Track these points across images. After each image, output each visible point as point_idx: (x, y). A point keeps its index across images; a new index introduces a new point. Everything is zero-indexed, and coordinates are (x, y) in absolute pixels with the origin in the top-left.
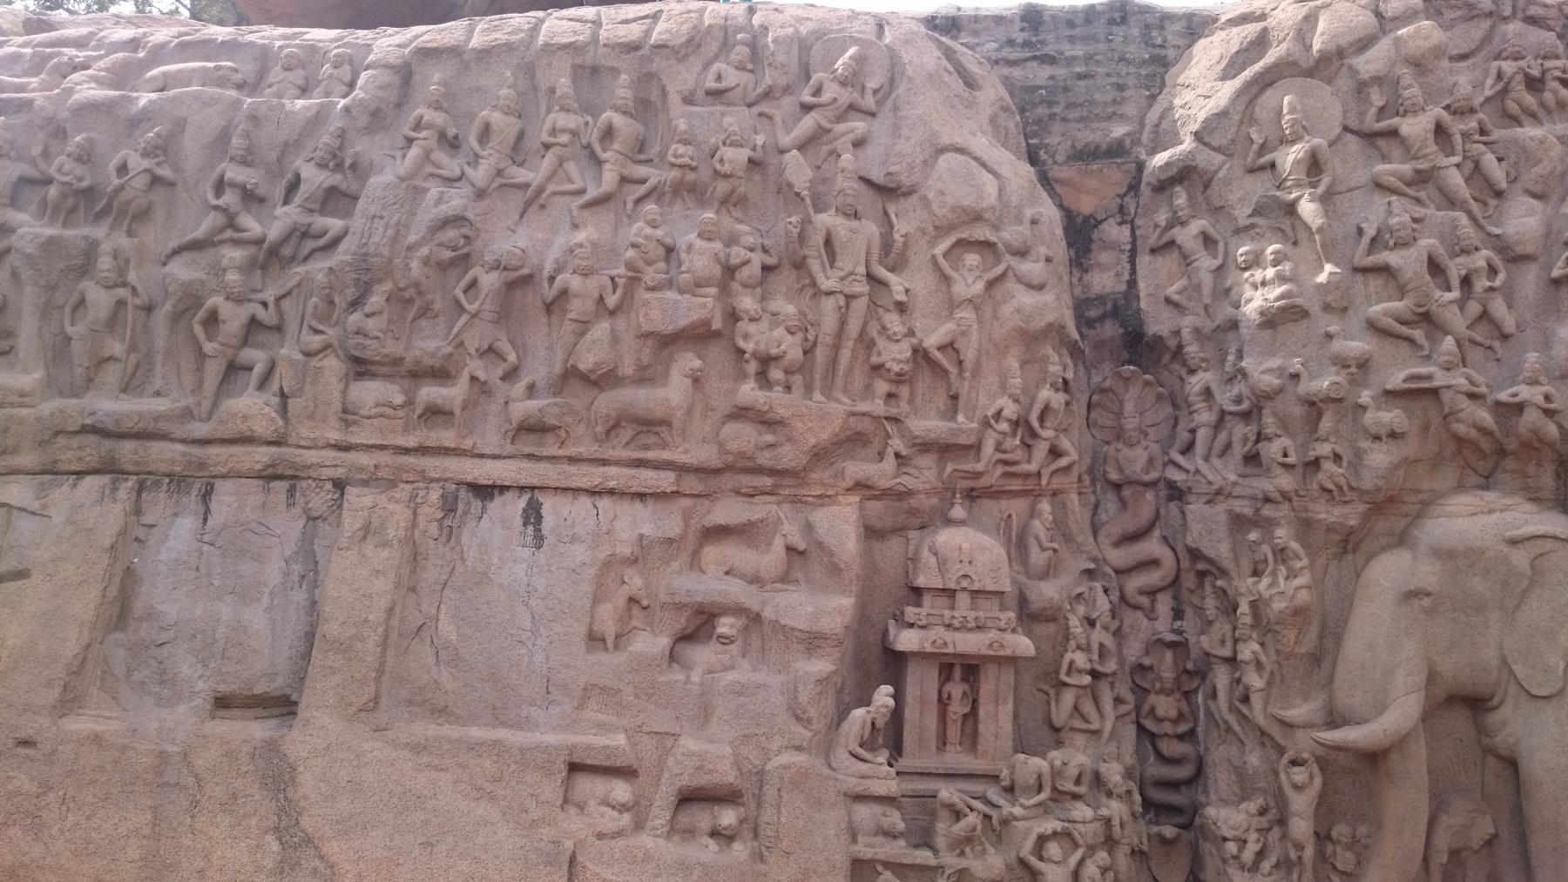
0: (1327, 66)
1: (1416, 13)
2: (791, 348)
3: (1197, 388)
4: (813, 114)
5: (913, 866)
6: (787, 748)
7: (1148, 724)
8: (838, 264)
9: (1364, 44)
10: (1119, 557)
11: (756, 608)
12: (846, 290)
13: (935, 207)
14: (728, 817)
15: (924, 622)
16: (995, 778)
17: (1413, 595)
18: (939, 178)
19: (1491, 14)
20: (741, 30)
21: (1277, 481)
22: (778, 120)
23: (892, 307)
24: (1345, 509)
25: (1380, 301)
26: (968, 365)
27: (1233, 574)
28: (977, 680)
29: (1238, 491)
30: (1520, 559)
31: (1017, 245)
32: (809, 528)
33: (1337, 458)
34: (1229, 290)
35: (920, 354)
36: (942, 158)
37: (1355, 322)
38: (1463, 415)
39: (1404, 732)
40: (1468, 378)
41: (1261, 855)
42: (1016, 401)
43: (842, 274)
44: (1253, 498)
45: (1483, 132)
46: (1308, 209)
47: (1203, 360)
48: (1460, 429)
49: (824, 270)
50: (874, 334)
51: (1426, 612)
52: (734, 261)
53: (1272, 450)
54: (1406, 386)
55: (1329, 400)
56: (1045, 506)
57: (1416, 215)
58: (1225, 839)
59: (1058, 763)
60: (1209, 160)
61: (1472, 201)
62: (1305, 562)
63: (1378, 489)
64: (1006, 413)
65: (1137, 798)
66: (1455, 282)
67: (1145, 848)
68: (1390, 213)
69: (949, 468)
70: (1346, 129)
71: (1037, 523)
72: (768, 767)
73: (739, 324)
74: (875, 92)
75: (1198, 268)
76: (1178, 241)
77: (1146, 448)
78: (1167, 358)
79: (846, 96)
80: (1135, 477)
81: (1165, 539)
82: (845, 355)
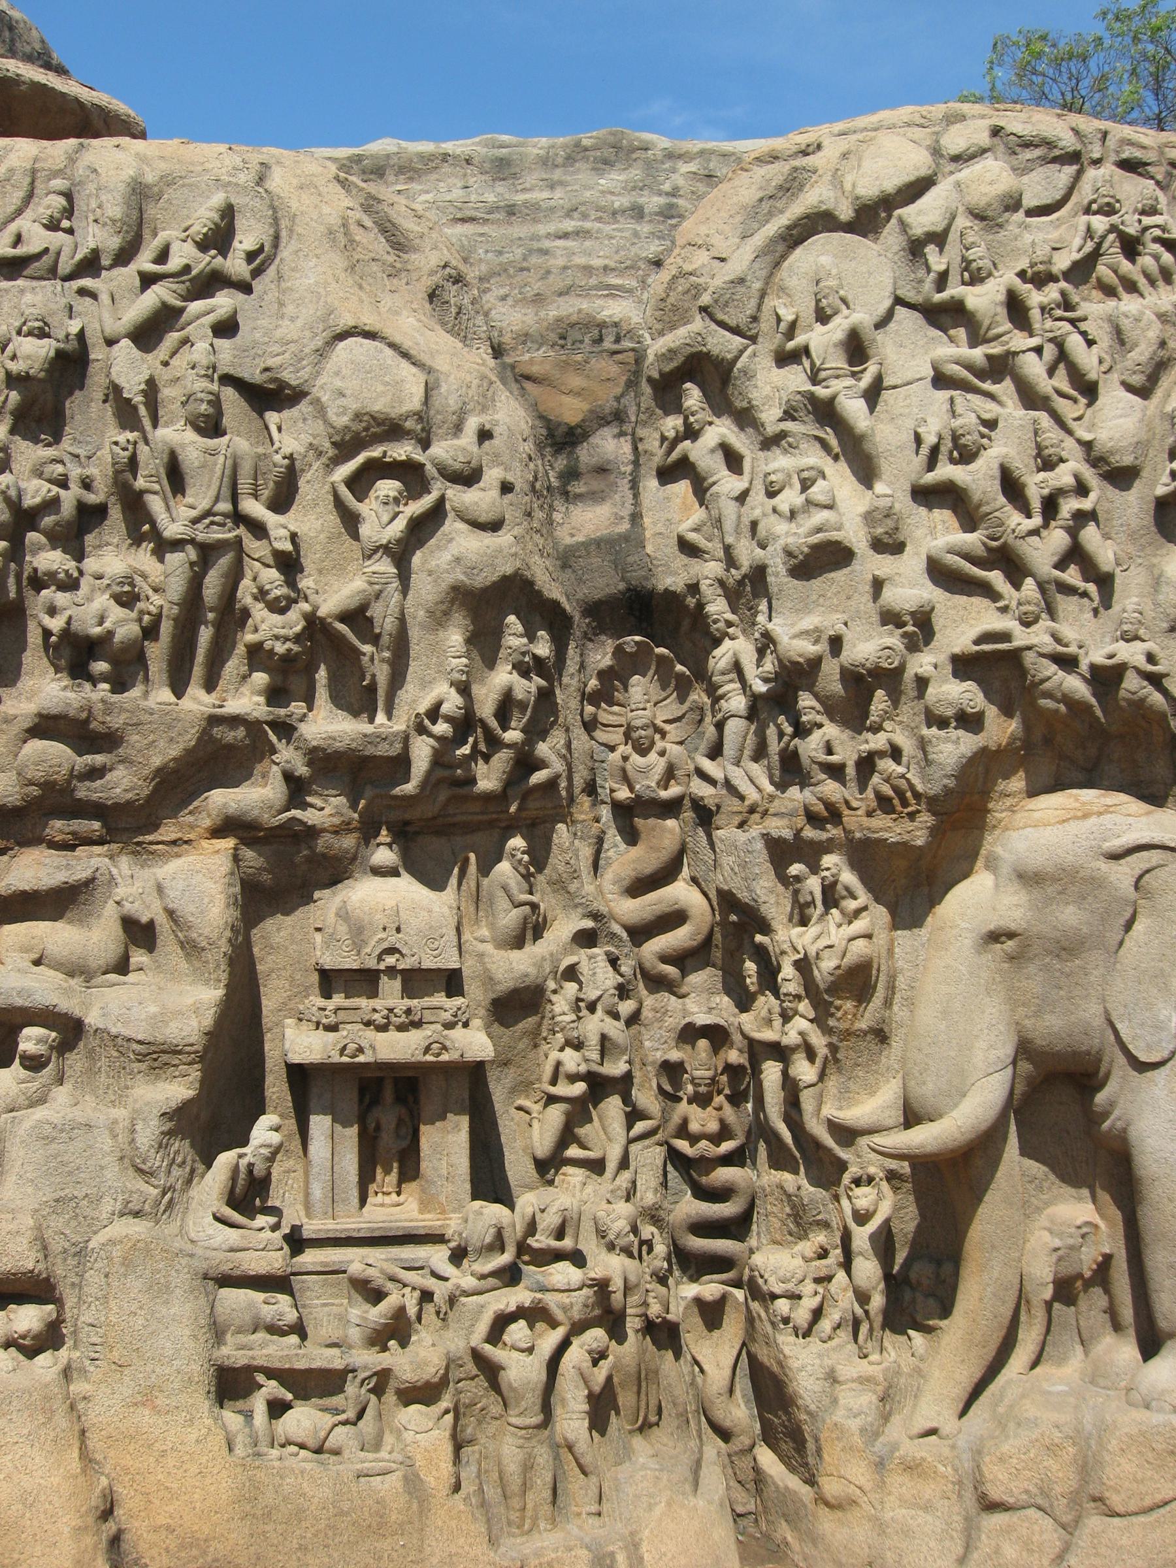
0: (868, 218)
1: (984, 151)
2: (123, 625)
3: (723, 664)
4: (155, 288)
5: (309, 1371)
6: (122, 1215)
7: (682, 1145)
8: (189, 500)
9: (917, 189)
10: (633, 909)
11: (77, 1012)
12: (201, 537)
13: (331, 414)
14: (27, 1318)
15: (332, 1020)
16: (437, 1239)
17: (994, 937)
18: (337, 374)
19: (1074, 157)
20: (56, 174)
21: (818, 789)
22: (104, 298)
23: (271, 561)
24: (910, 825)
26: (385, 640)
28: (416, 1101)
29: (775, 807)
30: (1122, 875)
31: (457, 466)
32: (160, 889)
33: (896, 753)
34: (754, 525)
35: (314, 625)
36: (342, 345)
38: (1047, 685)
39: (984, 1126)
41: (817, 1314)
42: (464, 689)
43: (194, 513)
44: (791, 815)
45: (1068, 305)
46: (854, 408)
47: (729, 624)
49: (168, 509)
50: (248, 600)
51: (1011, 958)
52: (29, 502)
53: (811, 747)
56: (517, 842)
57: (986, 416)
58: (774, 1297)
59: (529, 1211)
60: (723, 343)
61: (1055, 396)
62: (863, 897)
63: (948, 791)
64: (445, 708)
65: (660, 1249)
68: (954, 414)
69: (369, 792)
70: (899, 301)
71: (504, 867)
72: (91, 1245)
73: (44, 592)
74: (251, 256)
75: (718, 495)
76: (693, 457)
77: (662, 754)
78: (686, 623)
79: (203, 262)
80: (647, 794)
81: (694, 880)
82: (205, 635)
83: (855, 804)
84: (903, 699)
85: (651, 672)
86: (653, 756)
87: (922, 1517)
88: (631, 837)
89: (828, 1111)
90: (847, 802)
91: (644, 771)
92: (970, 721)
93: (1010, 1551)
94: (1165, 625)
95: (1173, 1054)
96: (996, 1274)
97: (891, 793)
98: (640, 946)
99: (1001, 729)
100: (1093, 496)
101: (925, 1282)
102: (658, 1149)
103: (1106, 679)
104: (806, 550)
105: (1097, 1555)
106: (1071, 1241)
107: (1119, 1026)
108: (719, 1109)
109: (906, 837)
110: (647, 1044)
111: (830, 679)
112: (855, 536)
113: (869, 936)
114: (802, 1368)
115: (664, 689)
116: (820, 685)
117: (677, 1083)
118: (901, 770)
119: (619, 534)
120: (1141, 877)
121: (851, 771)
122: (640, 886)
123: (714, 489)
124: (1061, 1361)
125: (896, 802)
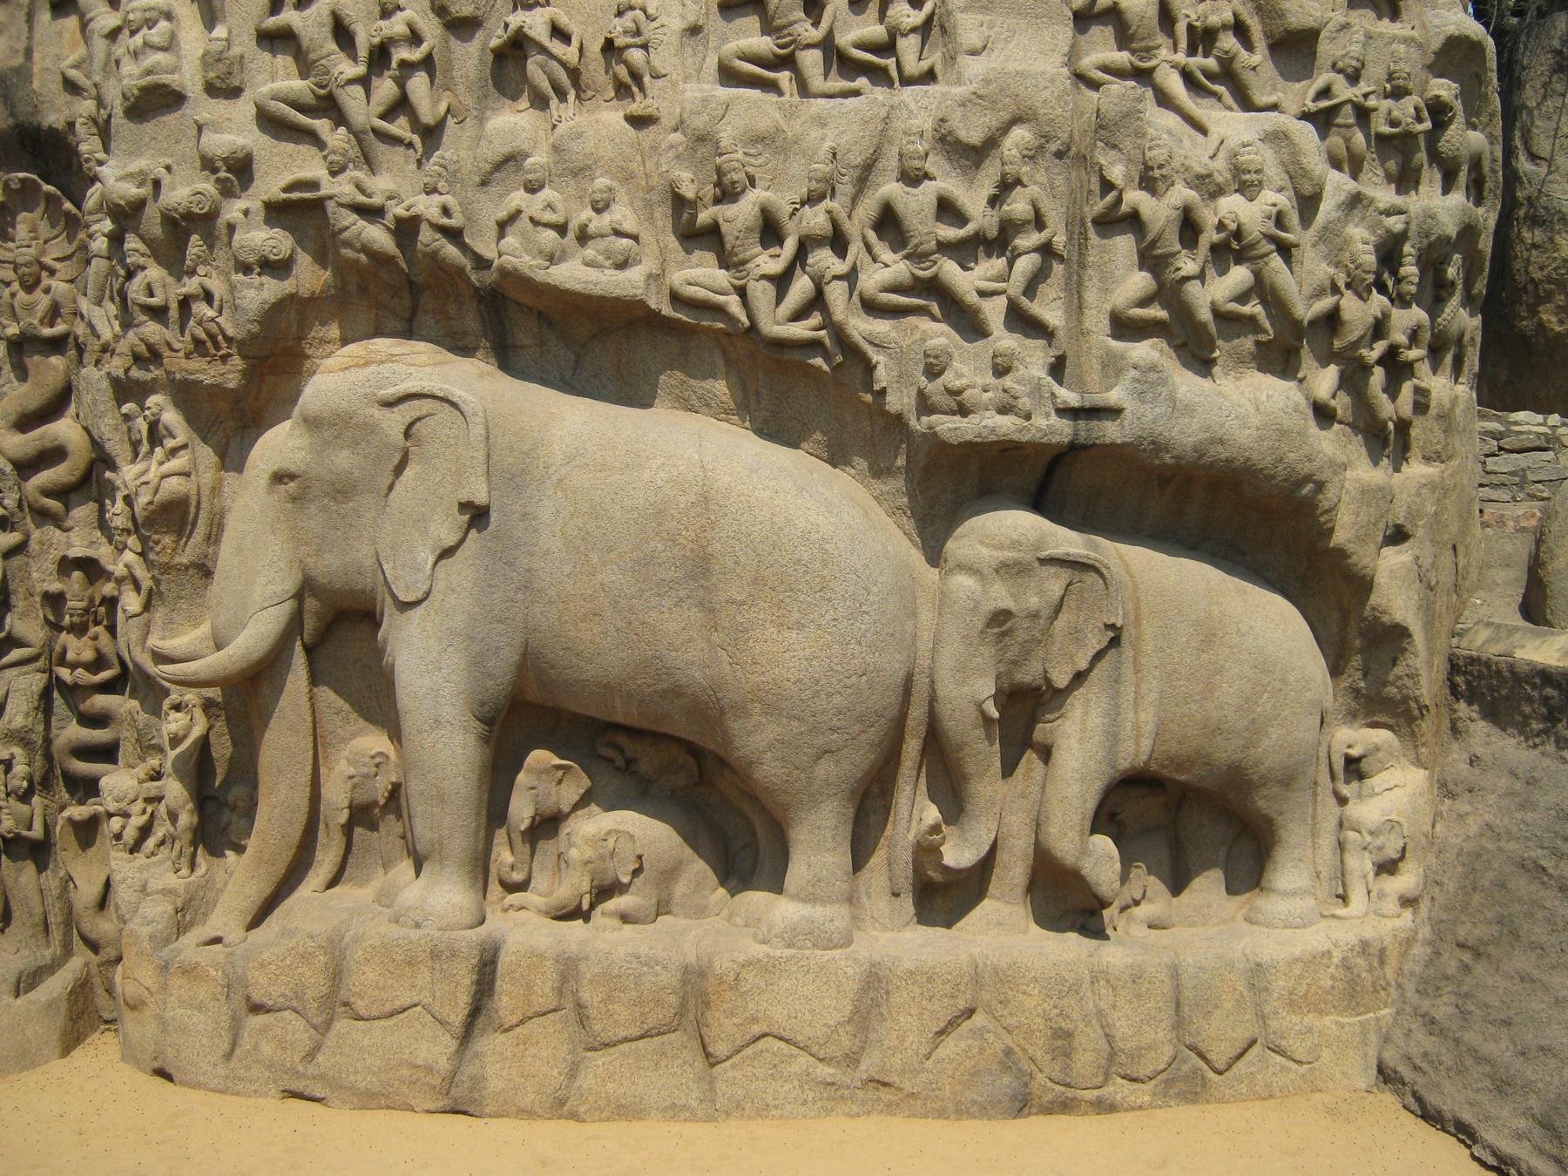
17: (279, 478)
21: (141, 330)
24: (222, 369)
25: (288, 77)
27: (119, 461)
33: (208, 297)
34: (118, 63)
37: (243, 109)
39: (255, 657)
40: (360, 187)
41: (145, 831)
48: (347, 253)
53: (135, 289)
54: (284, 196)
55: (189, 216)
63: (253, 337)
66: (363, 53)
67: (37, 832)
77: (47, 291)
83: (177, 346)
84: (218, 244)
85: (41, 209)
86: (38, 293)
87: (198, 1017)
88: (22, 373)
89: (154, 641)
90: (168, 344)
91: (29, 308)
92: (277, 267)
93: (267, 1049)
94: (477, 179)
95: (428, 594)
96: (282, 797)
97: (203, 336)
98: (26, 479)
99: (309, 276)
100: (424, 48)
101: (241, 804)
102: (39, 675)
103: (406, 229)
104: (136, 92)
105: (341, 1054)
106: (365, 770)
107: (385, 567)
108: (95, 638)
109: (220, 380)
110: (35, 575)
111: (152, 221)
112: (189, 79)
113: (188, 475)
114: (124, 881)
115: (53, 227)
116: (144, 227)
117: (59, 613)
118: (211, 313)
119: (11, 69)
120: (411, 425)
121: (174, 313)
122: (26, 422)
123: (92, 25)
124: (363, 883)
125: (209, 344)
